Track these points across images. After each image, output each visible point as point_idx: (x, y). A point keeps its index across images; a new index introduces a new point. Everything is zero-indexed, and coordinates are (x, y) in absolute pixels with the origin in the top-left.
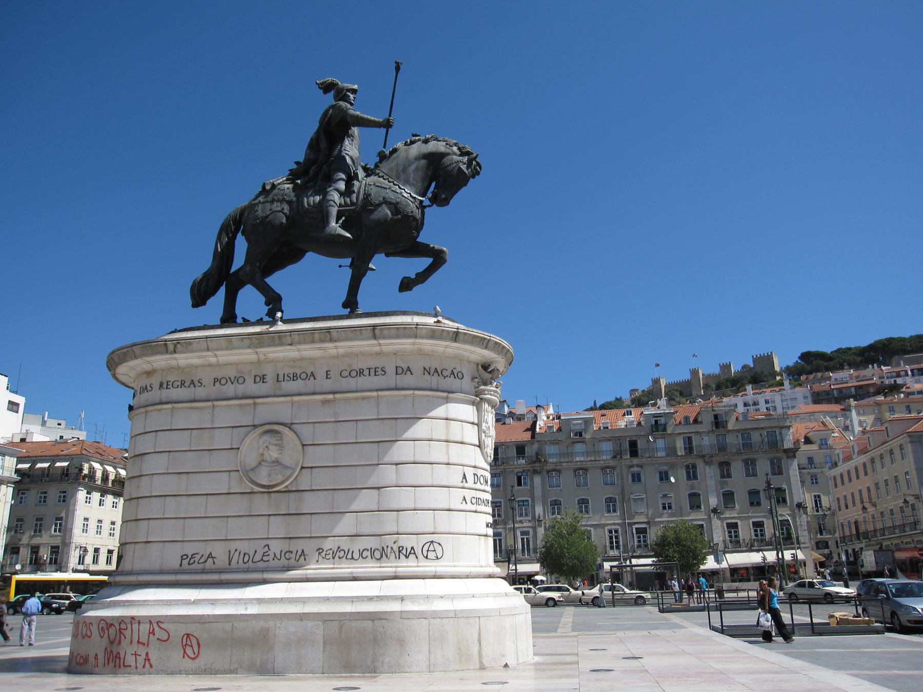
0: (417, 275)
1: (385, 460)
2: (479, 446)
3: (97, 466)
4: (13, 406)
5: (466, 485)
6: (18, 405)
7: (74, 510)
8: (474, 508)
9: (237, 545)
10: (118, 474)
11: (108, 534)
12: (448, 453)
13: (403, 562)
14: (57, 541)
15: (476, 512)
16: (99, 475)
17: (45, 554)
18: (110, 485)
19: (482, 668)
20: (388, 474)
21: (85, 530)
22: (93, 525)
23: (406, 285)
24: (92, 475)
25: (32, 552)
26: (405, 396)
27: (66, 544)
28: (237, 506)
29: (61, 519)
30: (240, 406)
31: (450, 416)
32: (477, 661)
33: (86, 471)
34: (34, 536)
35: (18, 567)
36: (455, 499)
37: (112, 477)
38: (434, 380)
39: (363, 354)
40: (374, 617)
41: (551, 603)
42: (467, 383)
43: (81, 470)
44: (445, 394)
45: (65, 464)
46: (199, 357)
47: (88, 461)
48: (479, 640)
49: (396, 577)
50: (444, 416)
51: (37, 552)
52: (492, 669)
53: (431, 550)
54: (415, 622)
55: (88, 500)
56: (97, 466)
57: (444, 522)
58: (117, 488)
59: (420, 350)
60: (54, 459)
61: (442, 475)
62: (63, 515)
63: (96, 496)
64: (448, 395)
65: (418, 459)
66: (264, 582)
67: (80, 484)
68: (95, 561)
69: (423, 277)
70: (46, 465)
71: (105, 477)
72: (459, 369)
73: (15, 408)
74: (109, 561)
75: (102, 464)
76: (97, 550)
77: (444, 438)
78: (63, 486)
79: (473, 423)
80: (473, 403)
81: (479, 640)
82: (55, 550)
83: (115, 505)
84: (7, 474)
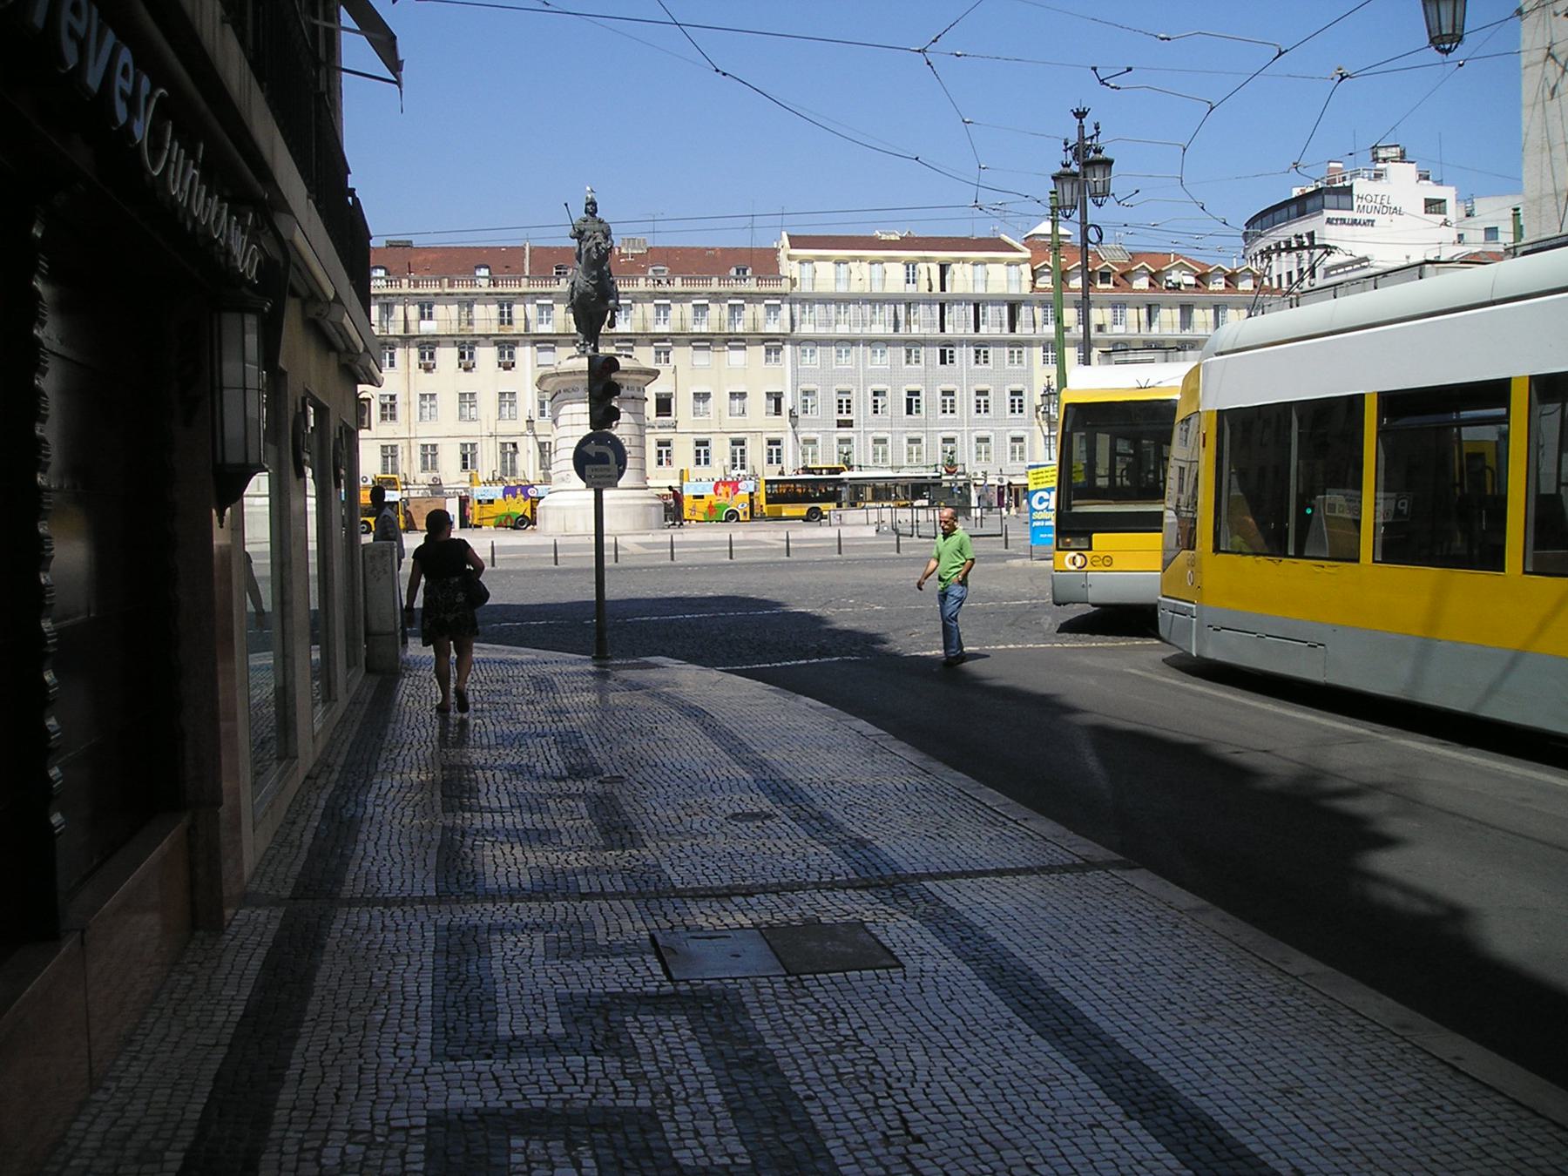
4: (1434, 206)
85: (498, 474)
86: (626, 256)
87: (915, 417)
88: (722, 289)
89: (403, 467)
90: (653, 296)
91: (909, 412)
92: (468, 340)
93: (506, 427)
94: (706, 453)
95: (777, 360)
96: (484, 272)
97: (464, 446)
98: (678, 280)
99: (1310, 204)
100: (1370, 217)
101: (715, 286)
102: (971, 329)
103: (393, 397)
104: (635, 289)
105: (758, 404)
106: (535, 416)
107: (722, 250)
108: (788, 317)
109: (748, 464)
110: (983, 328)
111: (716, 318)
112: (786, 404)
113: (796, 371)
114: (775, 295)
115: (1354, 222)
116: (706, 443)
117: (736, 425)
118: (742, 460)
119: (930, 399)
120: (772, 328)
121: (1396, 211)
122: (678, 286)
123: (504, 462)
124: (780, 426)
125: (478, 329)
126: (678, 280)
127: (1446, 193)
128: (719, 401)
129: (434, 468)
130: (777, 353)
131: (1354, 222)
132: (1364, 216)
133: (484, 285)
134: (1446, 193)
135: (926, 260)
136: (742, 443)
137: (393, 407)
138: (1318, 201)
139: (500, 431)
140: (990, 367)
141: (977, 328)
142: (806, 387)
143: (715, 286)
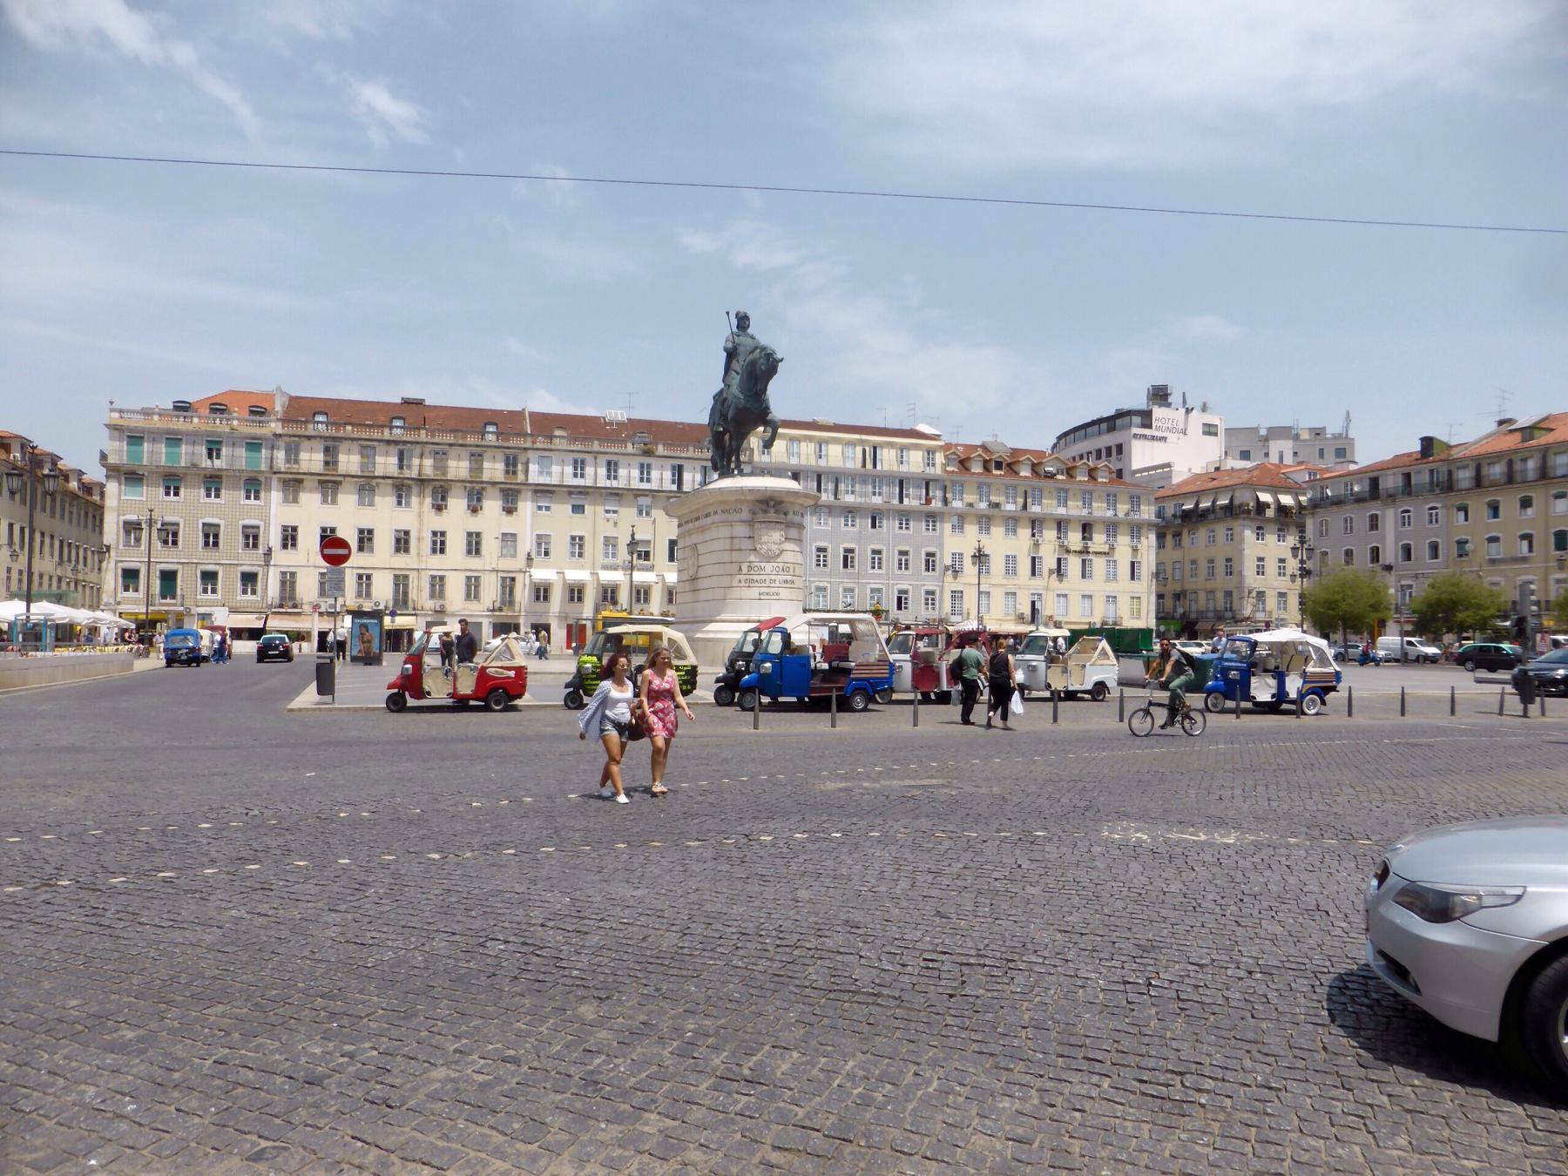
38: (726, 517)
85: (498, 605)
86: (611, 424)
87: (849, 570)
89: (413, 594)
91: (845, 566)
92: (478, 487)
93: (507, 564)
96: (491, 429)
97: (469, 578)
99: (1119, 422)
102: (896, 501)
103: (407, 533)
106: (533, 555)
110: (906, 501)
115: (1153, 438)
119: (863, 556)
123: (503, 593)
125: (486, 477)
129: (442, 595)
131: (1153, 438)
132: (1159, 434)
133: (491, 438)
135: (862, 442)
137: (407, 542)
138: (1127, 419)
139: (501, 567)
140: (911, 532)
141: (901, 501)
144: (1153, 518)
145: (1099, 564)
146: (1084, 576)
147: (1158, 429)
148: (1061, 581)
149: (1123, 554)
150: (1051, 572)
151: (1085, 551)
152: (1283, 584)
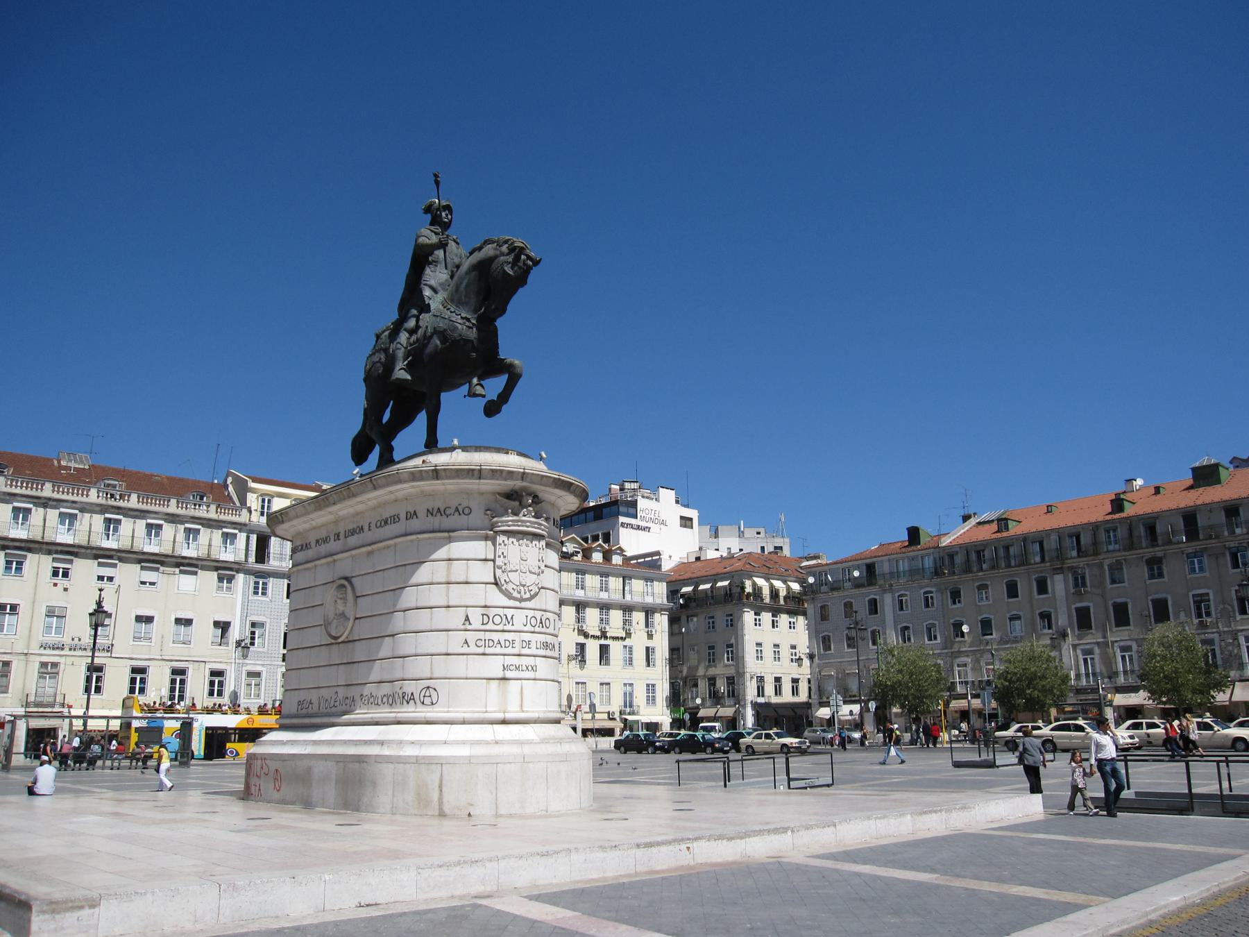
0: (499, 396)
1: (398, 607)
2: (496, 584)
3: (760, 582)
4: (686, 522)
5: (469, 627)
6: (691, 519)
7: (743, 636)
8: (480, 650)
9: (324, 692)
10: (789, 588)
11: (788, 660)
12: (447, 596)
13: (406, 708)
14: (731, 672)
15: (484, 654)
16: (766, 592)
17: (722, 687)
18: (782, 602)
19: (442, 815)
20: (398, 622)
21: (760, 657)
22: (768, 651)
23: (492, 409)
24: (757, 591)
25: (728, 684)
26: (412, 541)
27: (741, 674)
28: (322, 657)
29: (731, 646)
30: (328, 563)
31: (452, 556)
32: (437, 807)
33: (749, 589)
34: (709, 666)
35: (698, 701)
36: (454, 642)
37: (783, 593)
38: (436, 521)
39: (385, 503)
40: (360, 759)
41: (1240, 745)
42: (477, 517)
43: (743, 588)
44: (446, 534)
45: (726, 583)
46: (305, 522)
47: (750, 577)
48: (440, 787)
49: (399, 723)
50: (445, 557)
51: (714, 685)
52: (455, 817)
53: (428, 696)
54: (385, 765)
55: (757, 623)
56: (760, 582)
57: (441, 666)
58: (792, 606)
59: (422, 492)
60: (714, 578)
61: (441, 618)
62: (733, 641)
63: (766, 617)
64: (449, 534)
65: (420, 605)
66: (333, 725)
67: (744, 605)
68: (778, 691)
69: (504, 396)
70: (708, 586)
71: (774, 594)
72: (465, 504)
73: (688, 523)
74: (795, 691)
75: (767, 580)
76: (778, 680)
77: (444, 580)
78: (729, 608)
79: (486, 560)
80: (486, 538)
81: (440, 787)
82: (731, 681)
83: (792, 626)
84: (658, 601)
88: (180, 511)
90: (103, 509)
94: (143, 681)
95: (229, 589)
98: (134, 497)
100: (648, 525)
101: (173, 507)
104: (84, 499)
105: (204, 632)
107: (168, 478)
108: (243, 546)
109: (188, 694)
111: (170, 539)
112: (235, 633)
113: (246, 604)
114: (234, 525)
115: (639, 528)
116: (142, 671)
117: (178, 653)
118: (182, 691)
120: (227, 556)
121: (663, 523)
122: (133, 502)
124: (226, 657)
126: (134, 497)
127: (693, 513)
128: (163, 626)
130: (230, 581)
131: (639, 528)
132: (643, 524)
134: (693, 513)
136: (182, 672)
138: (614, 508)
142: (255, 618)
143: (173, 507)
144: (665, 601)
145: (616, 649)
146: (648, 665)
147: (643, 519)
148: (582, 668)
149: (639, 641)
150: (570, 658)
151: (604, 635)
152: (795, 671)
